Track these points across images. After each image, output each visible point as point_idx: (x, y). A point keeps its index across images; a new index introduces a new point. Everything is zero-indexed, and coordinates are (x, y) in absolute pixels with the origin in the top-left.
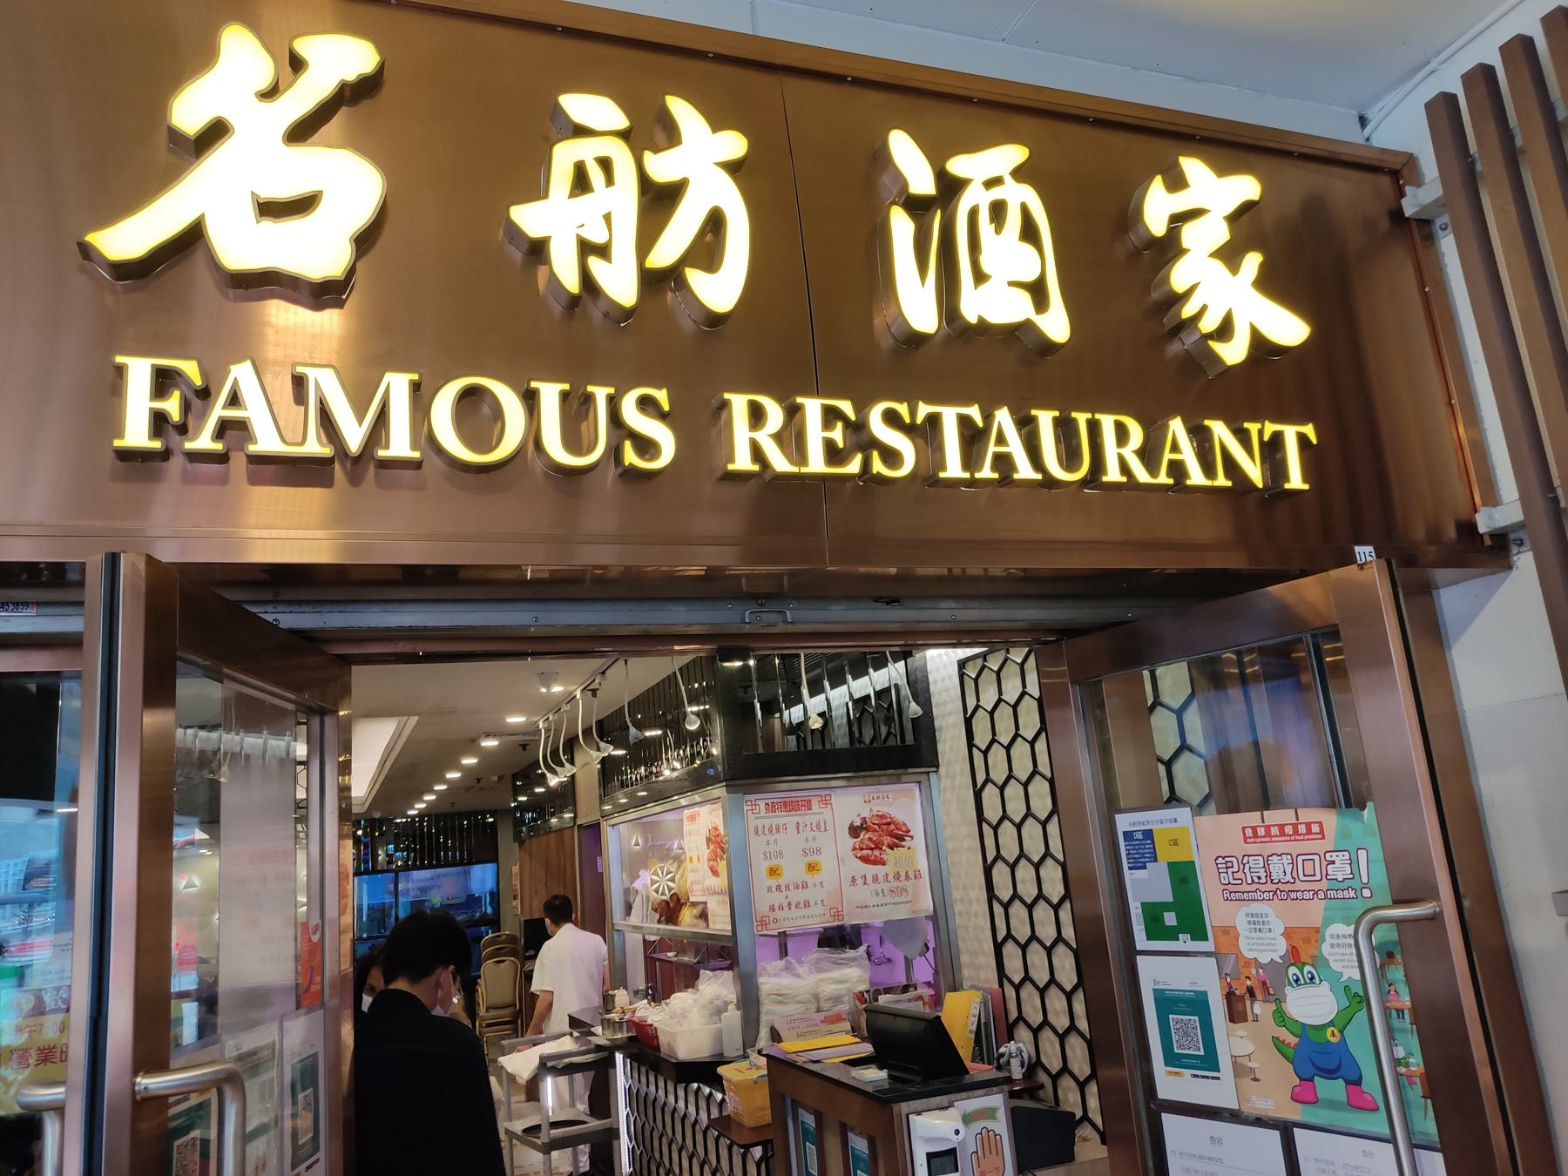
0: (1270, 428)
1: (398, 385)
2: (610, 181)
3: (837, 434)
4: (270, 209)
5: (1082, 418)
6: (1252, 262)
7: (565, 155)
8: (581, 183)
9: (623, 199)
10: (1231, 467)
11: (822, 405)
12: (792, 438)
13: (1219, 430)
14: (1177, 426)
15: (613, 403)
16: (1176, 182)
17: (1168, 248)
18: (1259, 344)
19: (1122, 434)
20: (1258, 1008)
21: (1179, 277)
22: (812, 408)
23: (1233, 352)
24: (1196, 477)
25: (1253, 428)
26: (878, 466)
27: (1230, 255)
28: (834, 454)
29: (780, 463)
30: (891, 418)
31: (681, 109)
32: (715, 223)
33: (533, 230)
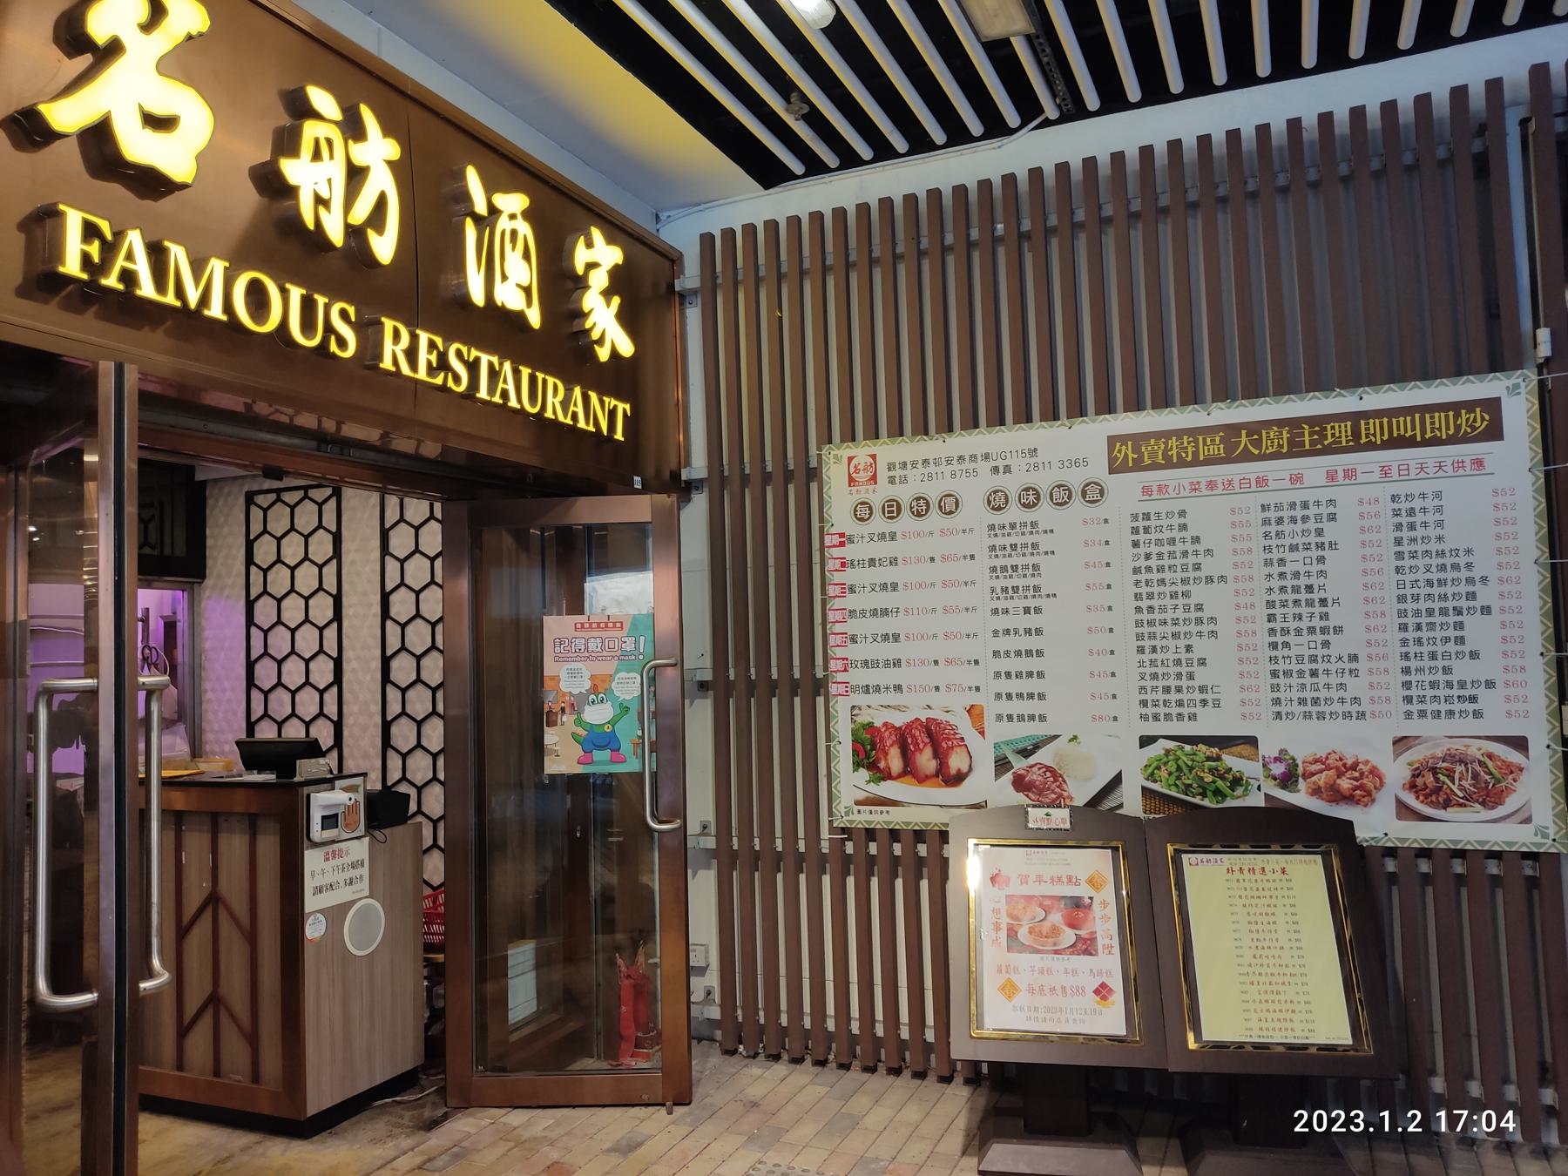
0: (614, 402)
1: (217, 267)
2: (331, 157)
3: (434, 358)
6: (616, 301)
8: (317, 155)
11: (83, 218)
13: (593, 396)
14: (577, 391)
15: (327, 307)
18: (614, 354)
20: (565, 718)
25: (606, 400)
26: (450, 383)
28: (431, 370)
30: (459, 354)
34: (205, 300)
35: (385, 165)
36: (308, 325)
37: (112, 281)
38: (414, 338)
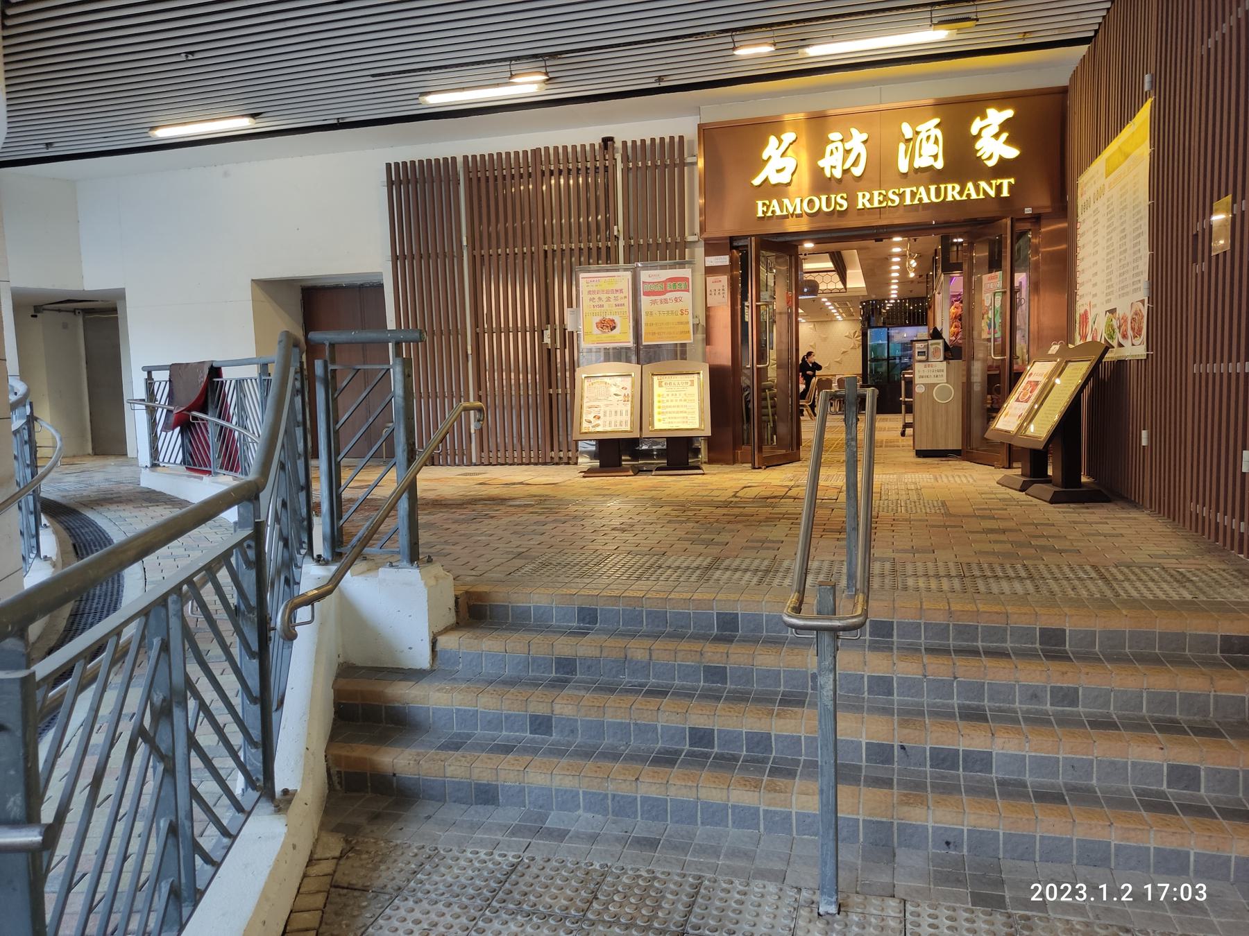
0: (999, 181)
3: (881, 198)
4: (778, 171)
5: (942, 186)
6: (1005, 136)
7: (829, 148)
9: (839, 155)
10: (985, 192)
12: (870, 201)
13: (983, 184)
16: (984, 116)
17: (978, 136)
19: (953, 188)
21: (978, 146)
22: (876, 193)
23: (991, 163)
24: (974, 196)
25: (994, 182)
27: (997, 136)
28: (880, 202)
29: (868, 205)
30: (894, 193)
31: (854, 131)
32: (859, 155)
33: (822, 166)
34: (795, 210)
35: (862, 145)
36: (828, 205)
37: (769, 214)
38: (872, 195)
